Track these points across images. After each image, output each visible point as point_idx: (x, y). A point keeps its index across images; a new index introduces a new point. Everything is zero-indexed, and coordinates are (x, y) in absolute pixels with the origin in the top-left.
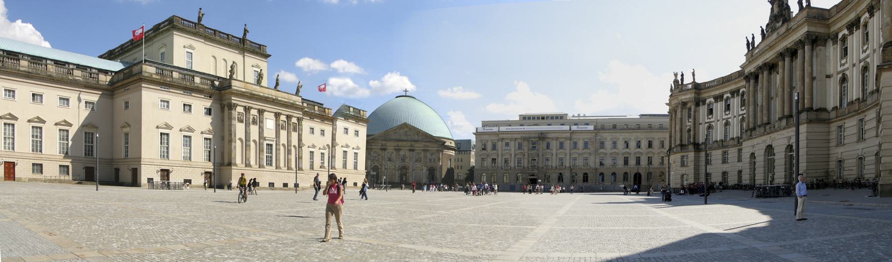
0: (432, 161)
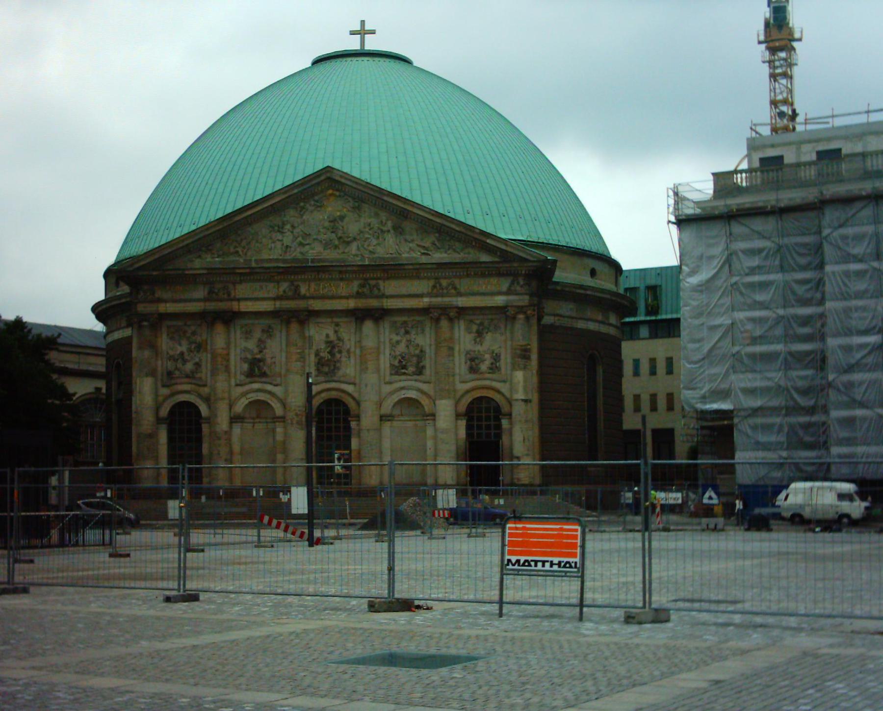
0: (484, 367)
